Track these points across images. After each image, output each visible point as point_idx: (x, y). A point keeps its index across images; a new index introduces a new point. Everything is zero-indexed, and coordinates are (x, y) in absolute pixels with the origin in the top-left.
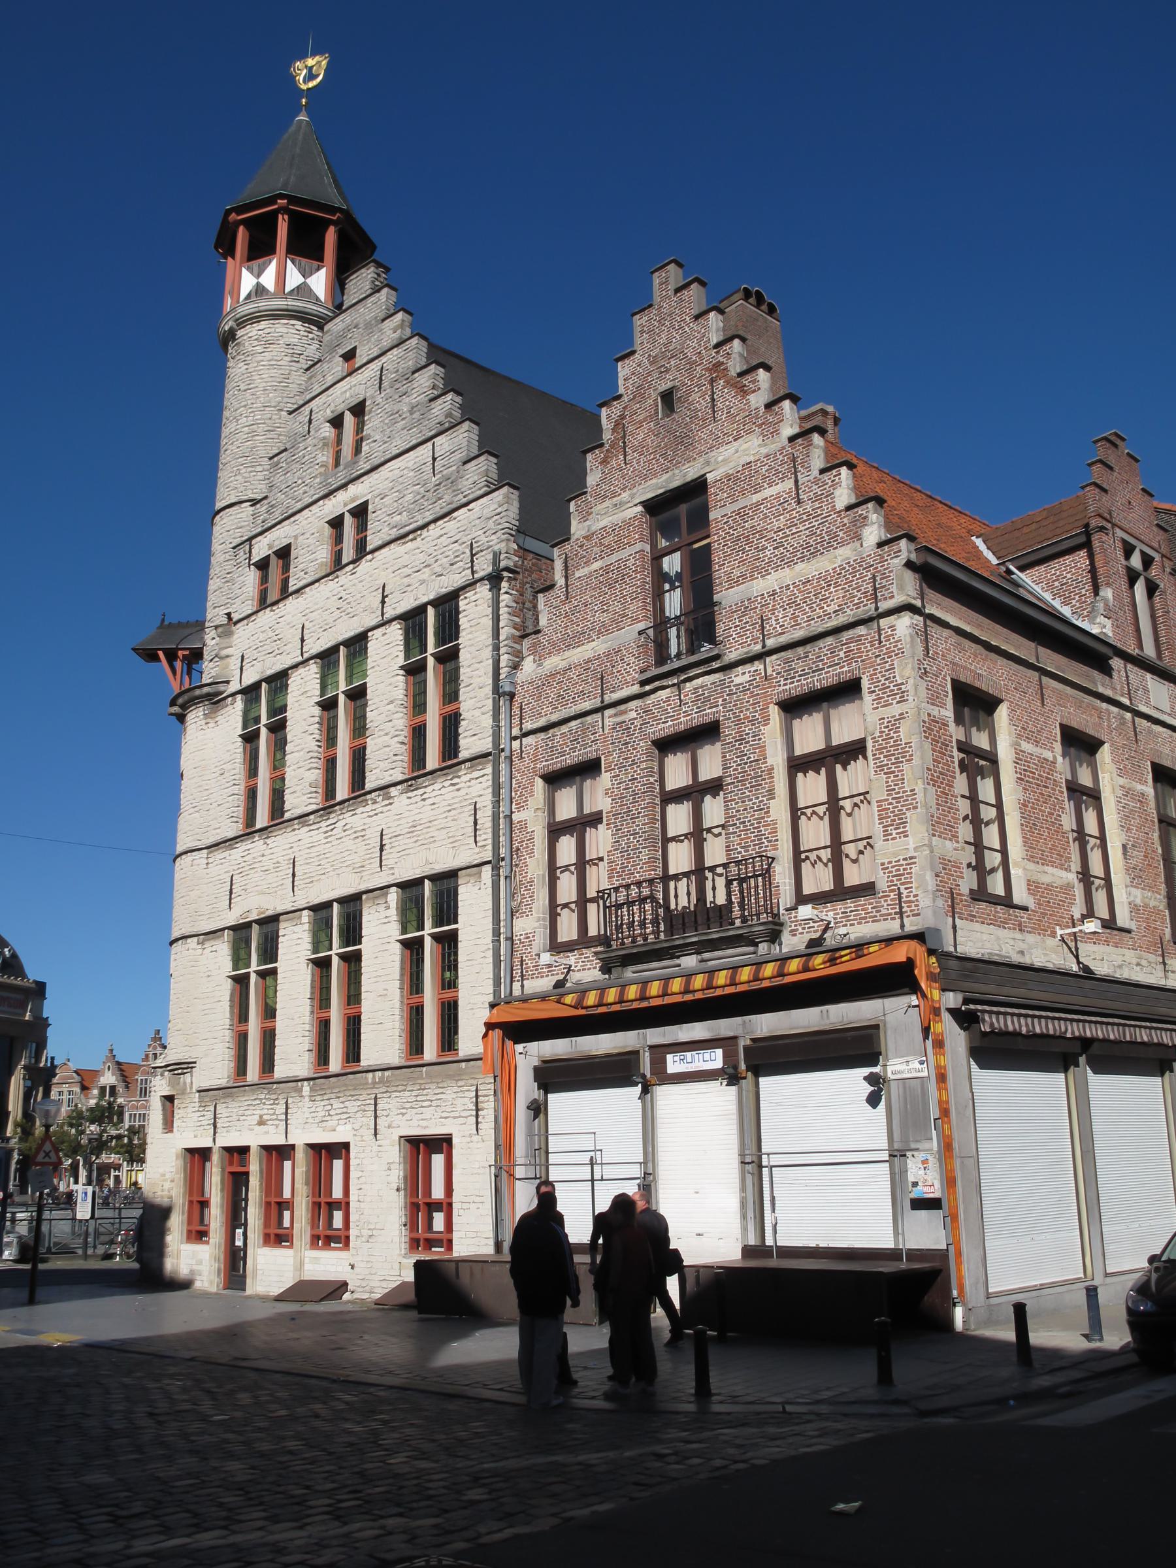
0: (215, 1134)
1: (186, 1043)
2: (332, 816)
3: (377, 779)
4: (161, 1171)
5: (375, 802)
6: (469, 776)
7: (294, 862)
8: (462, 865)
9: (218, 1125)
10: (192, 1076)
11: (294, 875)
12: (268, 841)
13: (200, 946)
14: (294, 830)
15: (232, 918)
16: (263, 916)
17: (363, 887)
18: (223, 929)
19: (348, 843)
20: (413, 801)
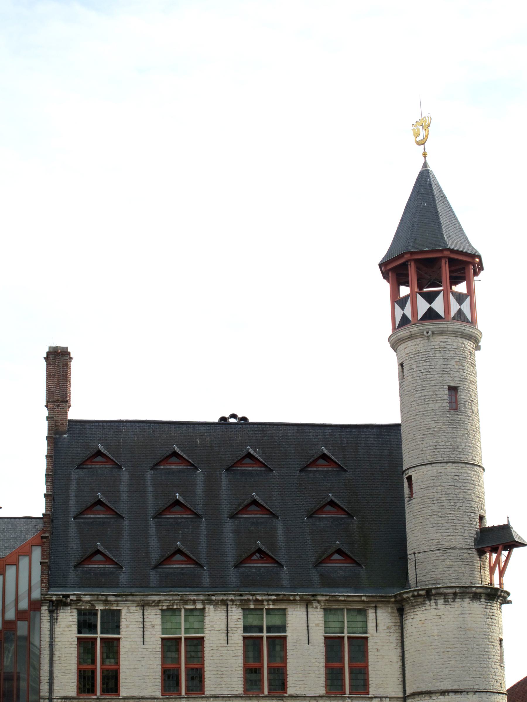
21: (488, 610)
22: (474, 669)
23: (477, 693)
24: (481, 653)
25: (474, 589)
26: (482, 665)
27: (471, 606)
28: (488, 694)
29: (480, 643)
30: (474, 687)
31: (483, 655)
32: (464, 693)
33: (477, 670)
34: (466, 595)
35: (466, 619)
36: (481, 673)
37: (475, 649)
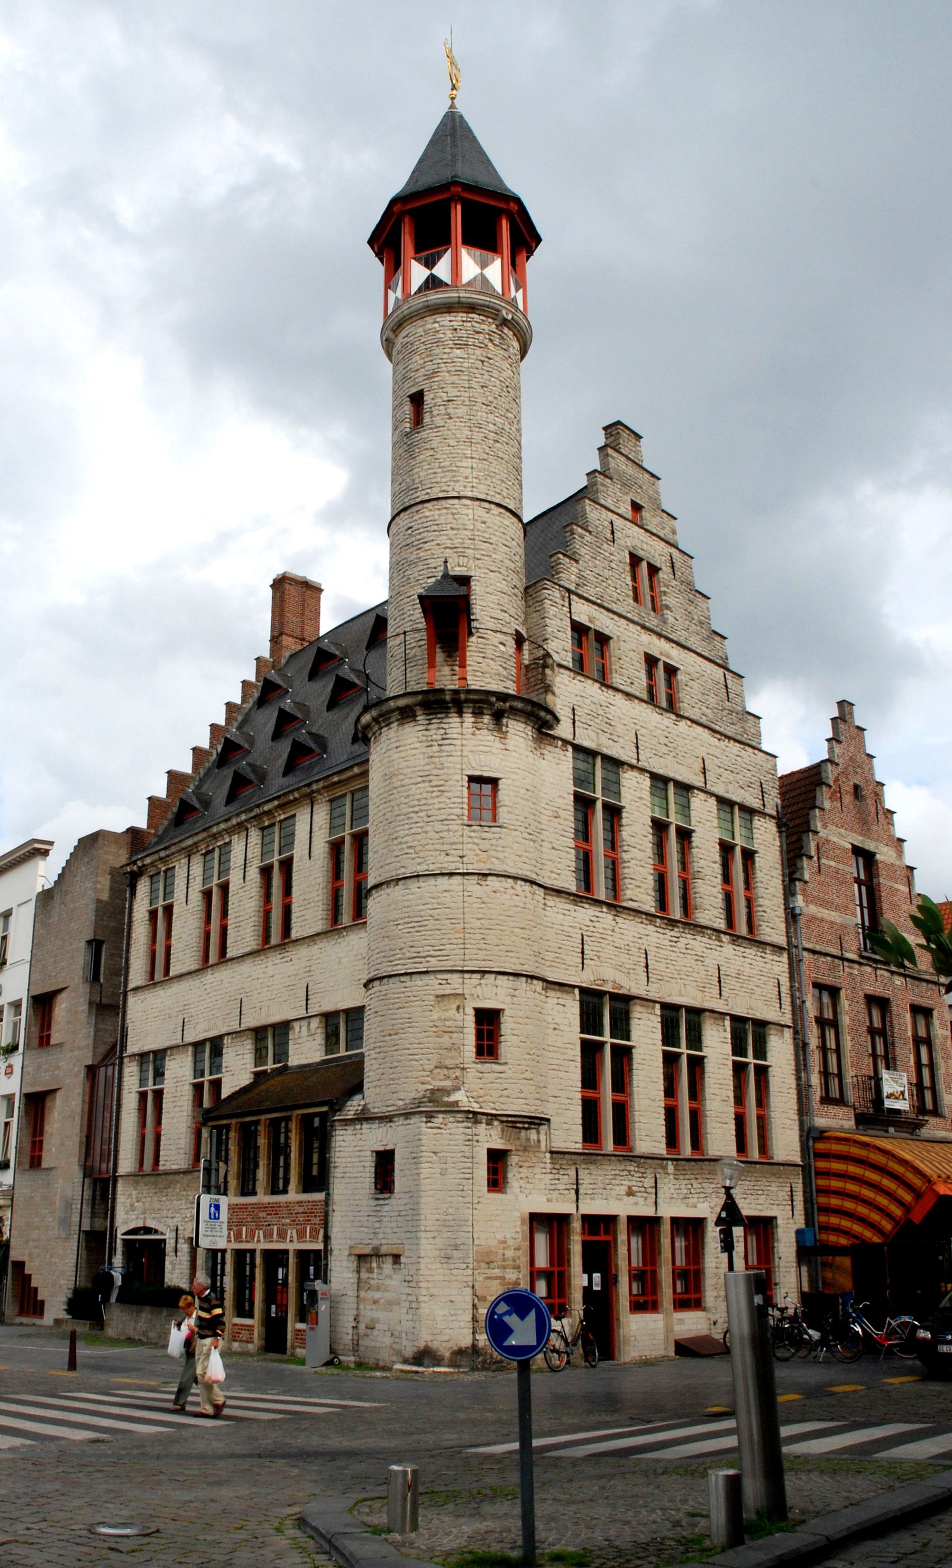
0: (577, 1201)
1: (538, 1096)
2: (676, 929)
3: (710, 920)
4: (500, 1236)
5: (710, 938)
6: (771, 957)
7: (646, 954)
8: (772, 1021)
9: (581, 1191)
10: (538, 1133)
11: (647, 966)
12: (618, 919)
13: (543, 992)
14: (642, 923)
15: (585, 979)
16: (616, 991)
17: (707, 1005)
18: (574, 987)
19: (690, 961)
20: (739, 953)
21: (432, 732)
22: (399, 840)
23: (401, 883)
24: (410, 810)
25: (392, 704)
26: (413, 831)
27: (400, 732)
28: (421, 879)
29: (411, 792)
30: (399, 872)
31: (417, 812)
32: (385, 886)
33: (403, 840)
34: (390, 718)
35: (391, 759)
36: (409, 844)
37: (402, 806)
